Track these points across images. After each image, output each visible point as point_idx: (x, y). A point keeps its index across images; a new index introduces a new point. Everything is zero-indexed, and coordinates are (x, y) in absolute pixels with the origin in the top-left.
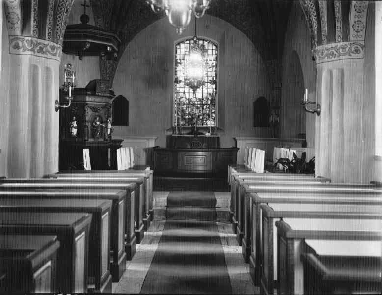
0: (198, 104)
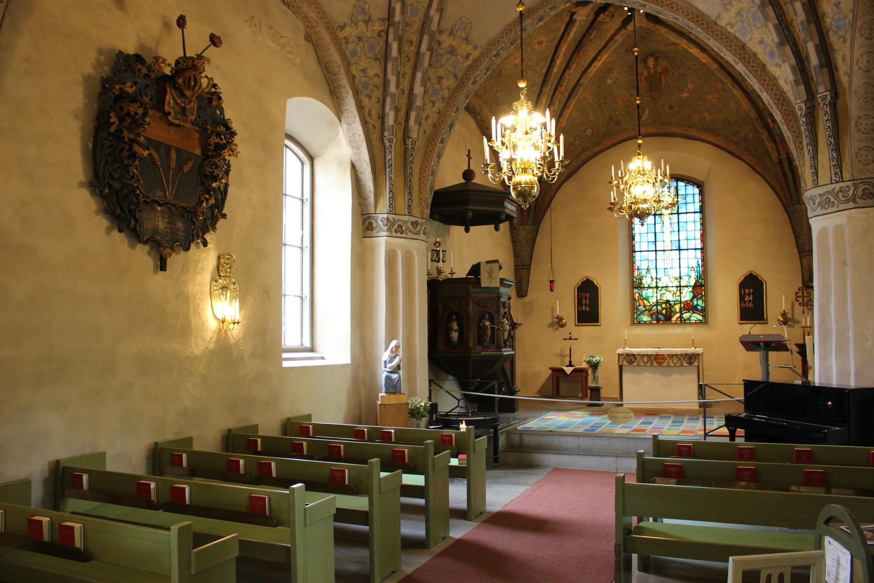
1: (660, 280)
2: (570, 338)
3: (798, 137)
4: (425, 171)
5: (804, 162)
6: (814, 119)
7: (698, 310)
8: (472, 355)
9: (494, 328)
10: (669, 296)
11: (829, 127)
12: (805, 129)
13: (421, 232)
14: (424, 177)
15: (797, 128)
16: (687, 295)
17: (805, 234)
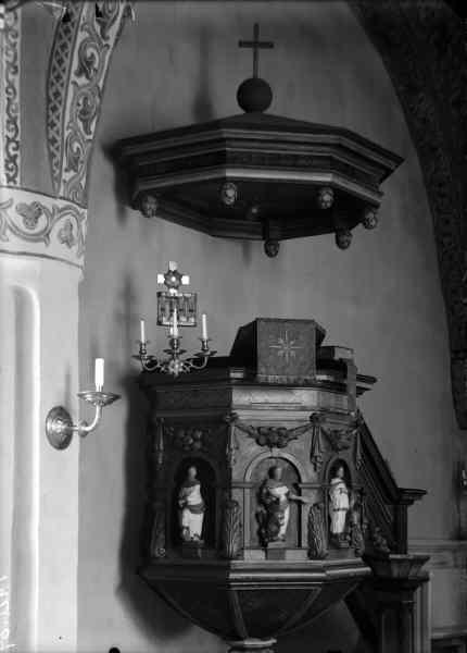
8: (232, 576)
13: (53, 235)
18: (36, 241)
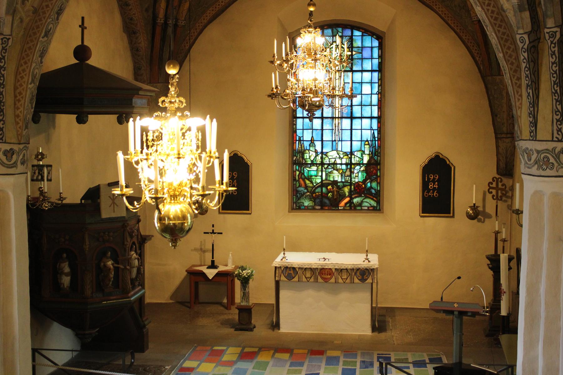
0: (341, 164)
1: (326, 156)
2: (213, 232)
3: (515, 71)
4: (22, 78)
5: (521, 104)
6: (538, 53)
7: (371, 194)
9: (118, 268)
10: (336, 176)
11: (556, 72)
12: (526, 67)
14: (21, 85)
15: (515, 59)
16: (359, 176)
17: (504, 112)
18: (12, 167)
